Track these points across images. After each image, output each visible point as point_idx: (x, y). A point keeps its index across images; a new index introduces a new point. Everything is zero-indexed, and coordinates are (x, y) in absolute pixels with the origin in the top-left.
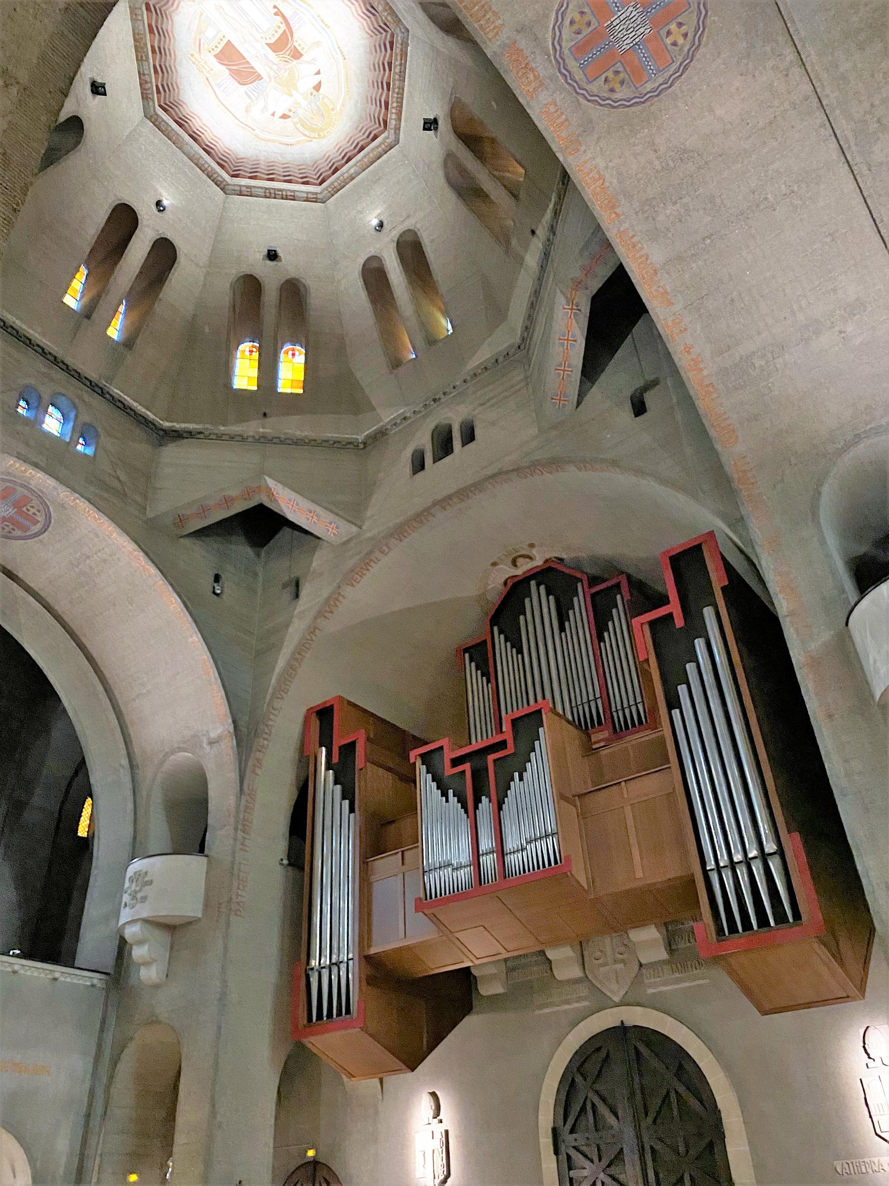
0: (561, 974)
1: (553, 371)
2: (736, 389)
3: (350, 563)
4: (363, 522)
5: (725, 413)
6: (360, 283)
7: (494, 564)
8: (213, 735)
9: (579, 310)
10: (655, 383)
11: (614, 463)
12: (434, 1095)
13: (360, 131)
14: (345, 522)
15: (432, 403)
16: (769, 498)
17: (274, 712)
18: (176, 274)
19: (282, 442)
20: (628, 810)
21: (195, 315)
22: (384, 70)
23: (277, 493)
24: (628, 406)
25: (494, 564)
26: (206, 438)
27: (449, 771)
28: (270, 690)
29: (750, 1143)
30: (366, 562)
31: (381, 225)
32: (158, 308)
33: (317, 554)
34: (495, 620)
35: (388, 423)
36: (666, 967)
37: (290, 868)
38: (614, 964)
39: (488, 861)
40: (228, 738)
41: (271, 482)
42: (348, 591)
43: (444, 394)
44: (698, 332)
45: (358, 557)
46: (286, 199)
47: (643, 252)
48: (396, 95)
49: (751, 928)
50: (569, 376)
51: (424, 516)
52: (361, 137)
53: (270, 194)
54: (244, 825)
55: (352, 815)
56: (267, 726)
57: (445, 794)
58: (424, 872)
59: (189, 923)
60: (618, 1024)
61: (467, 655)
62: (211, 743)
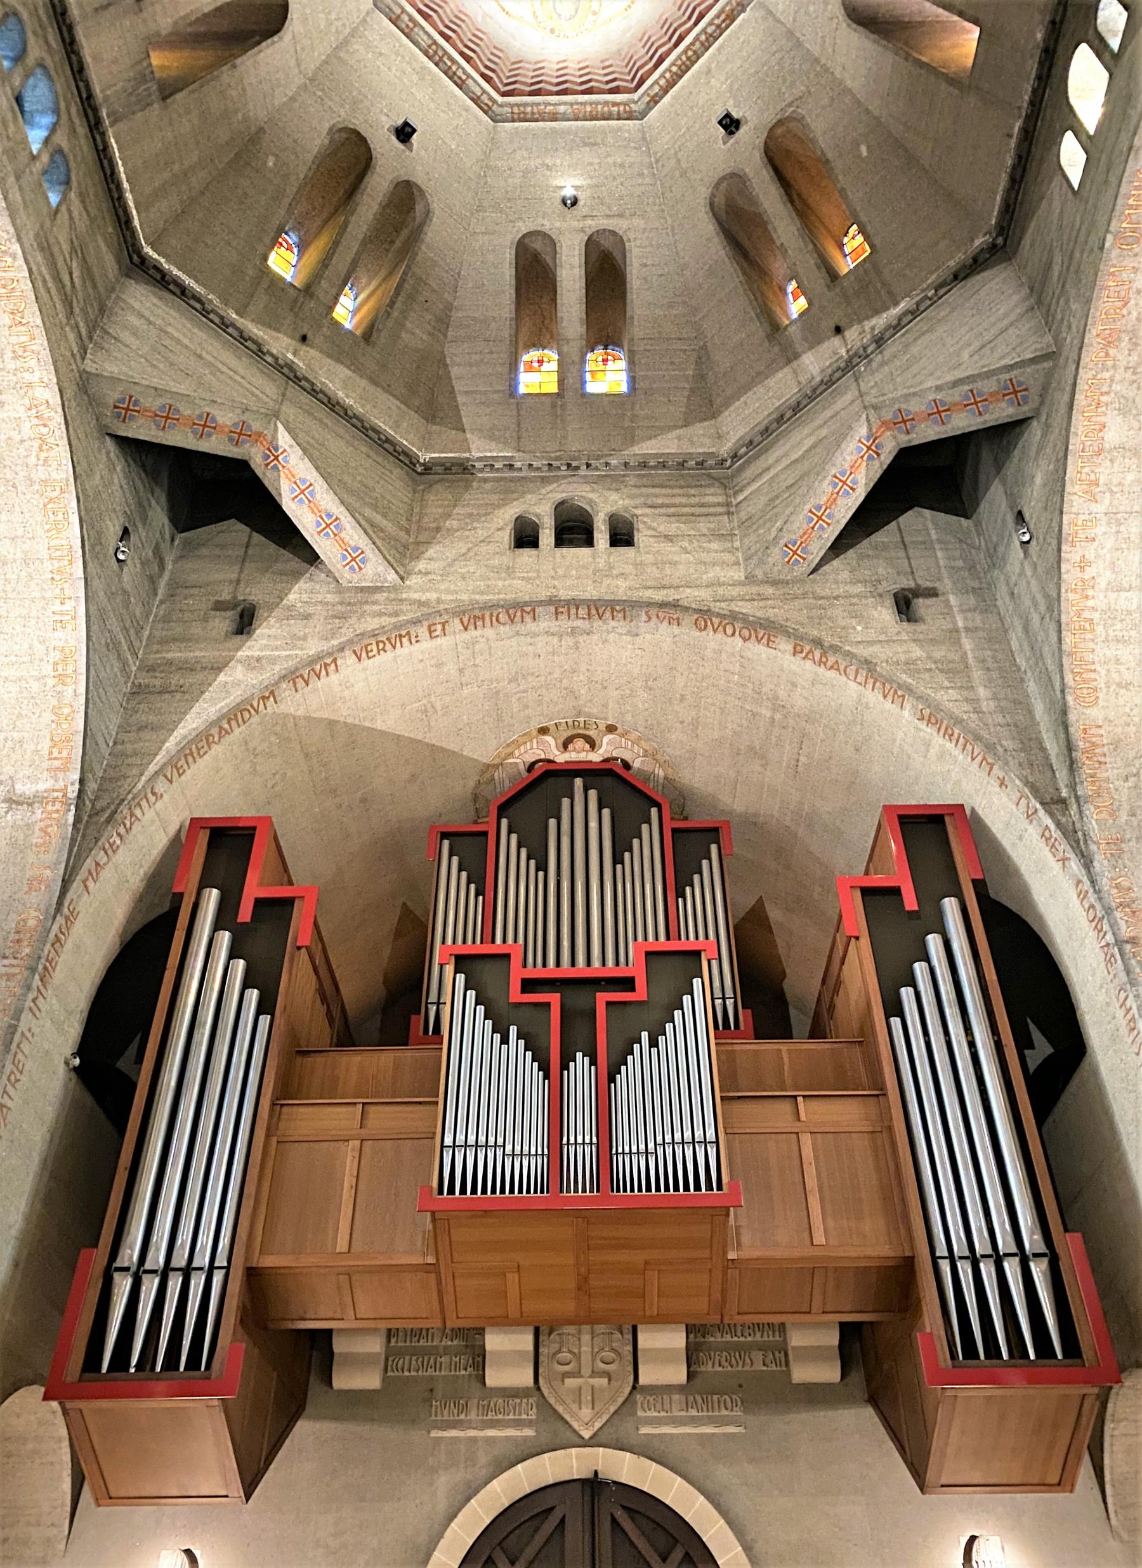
0: (495, 1378)
1: (806, 512)
2: (1118, 641)
3: (371, 624)
4: (409, 574)
5: (1094, 663)
7: (543, 731)
8: (24, 788)
9: (878, 455)
10: (932, 593)
12: (188, 1552)
13: (604, 68)
14: (381, 560)
15: (564, 468)
16: (1116, 790)
17: (150, 795)
18: (269, 51)
20: (806, 1140)
21: (261, 130)
22: (690, 18)
23: (287, 462)
24: (890, 602)
25: (543, 731)
26: (205, 312)
28: (160, 759)
30: (398, 635)
31: (575, 202)
32: (226, 75)
33: (302, 585)
35: (480, 459)
36: (676, 1397)
37: (73, 1075)
38: (591, 1377)
40: (58, 806)
41: (284, 439)
42: (348, 661)
43: (588, 465)
44: (1105, 551)
45: (394, 620)
46: (451, 78)
47: (1102, 419)
48: (684, 58)
49: (1000, 1356)
50: (822, 528)
51: (523, 611)
52: (599, 77)
53: (433, 54)
54: (45, 968)
55: (265, 1020)
56: (132, 815)
58: (442, 1147)
60: (586, 1474)
61: (446, 843)
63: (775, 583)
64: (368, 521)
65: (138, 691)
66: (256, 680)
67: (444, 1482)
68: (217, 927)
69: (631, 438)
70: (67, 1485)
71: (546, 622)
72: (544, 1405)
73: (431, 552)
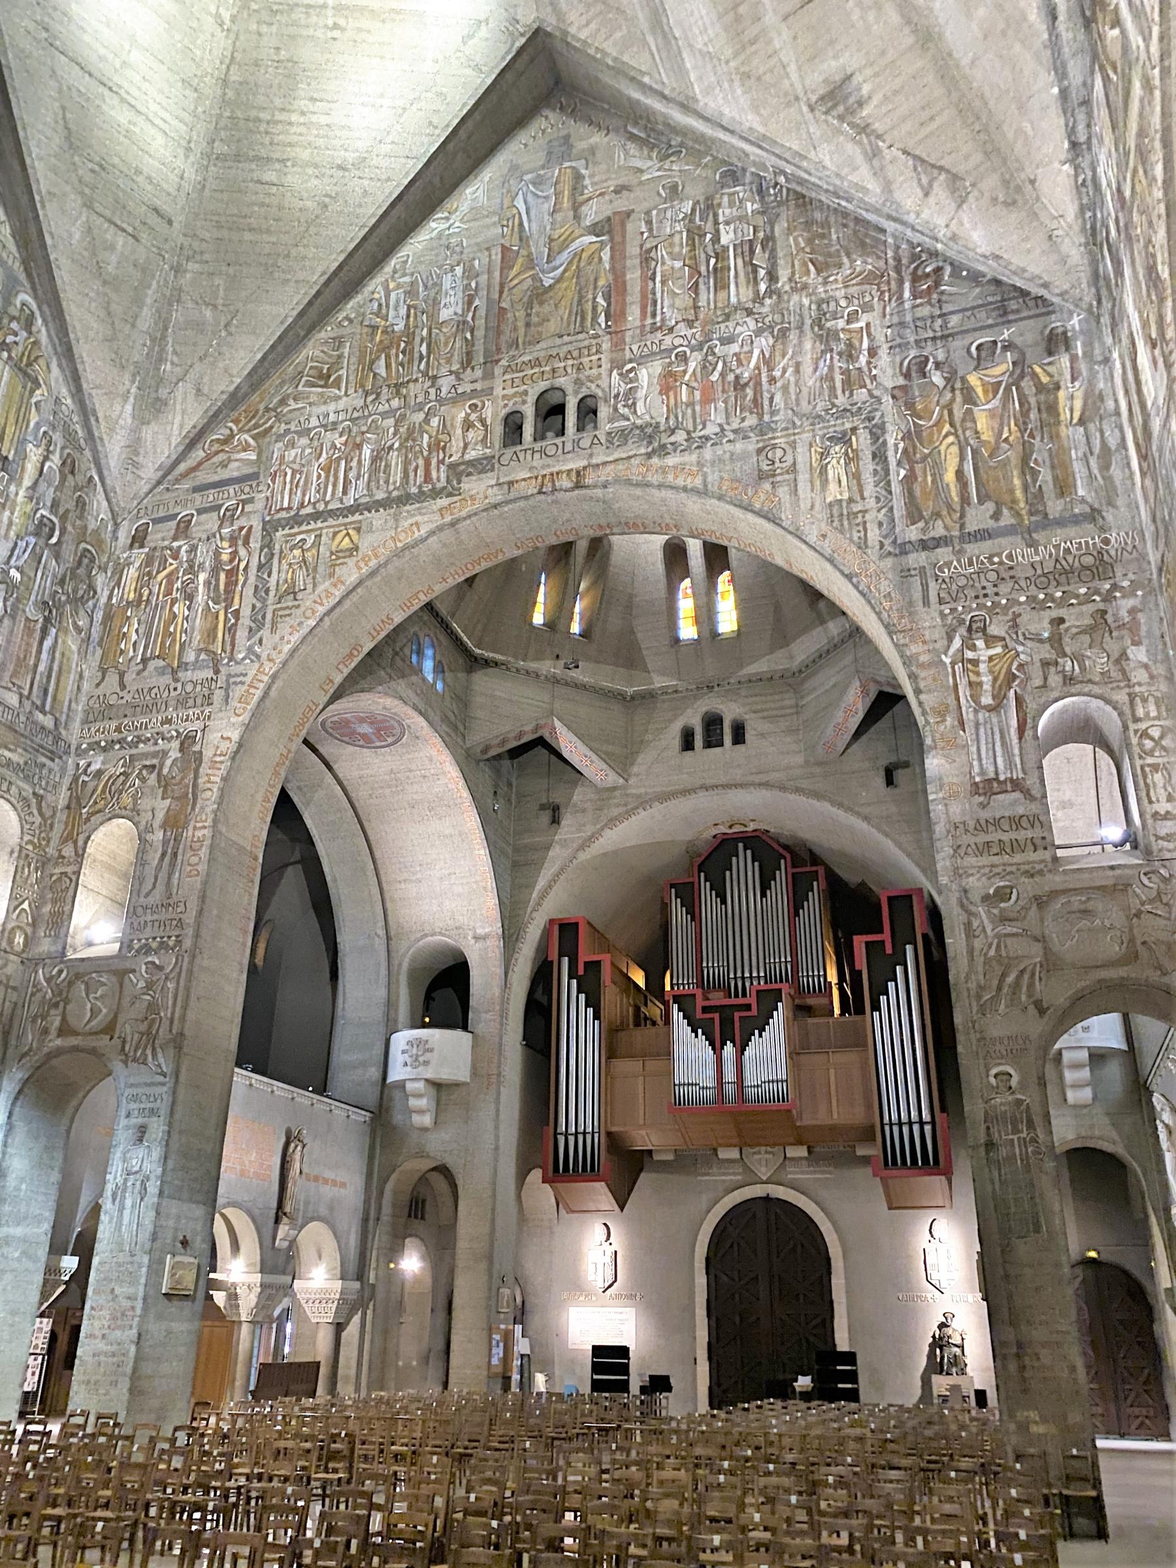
3: (615, 812)
6: (660, 555)
8: (480, 931)
10: (906, 765)
11: (866, 818)
19: (567, 684)
20: (832, 1071)
24: (883, 773)
26: (508, 669)
27: (699, 1015)
29: (846, 1278)
34: (701, 868)
39: (730, 1089)
41: (557, 723)
57: (694, 1031)
59: (457, 1085)
62: (477, 938)
63: (819, 764)
64: (606, 753)
65: (515, 865)
66: (566, 853)
67: (705, 1199)
68: (570, 977)
69: (742, 667)
70: (553, 1200)
71: (702, 793)
72: (745, 1166)
73: (639, 760)
